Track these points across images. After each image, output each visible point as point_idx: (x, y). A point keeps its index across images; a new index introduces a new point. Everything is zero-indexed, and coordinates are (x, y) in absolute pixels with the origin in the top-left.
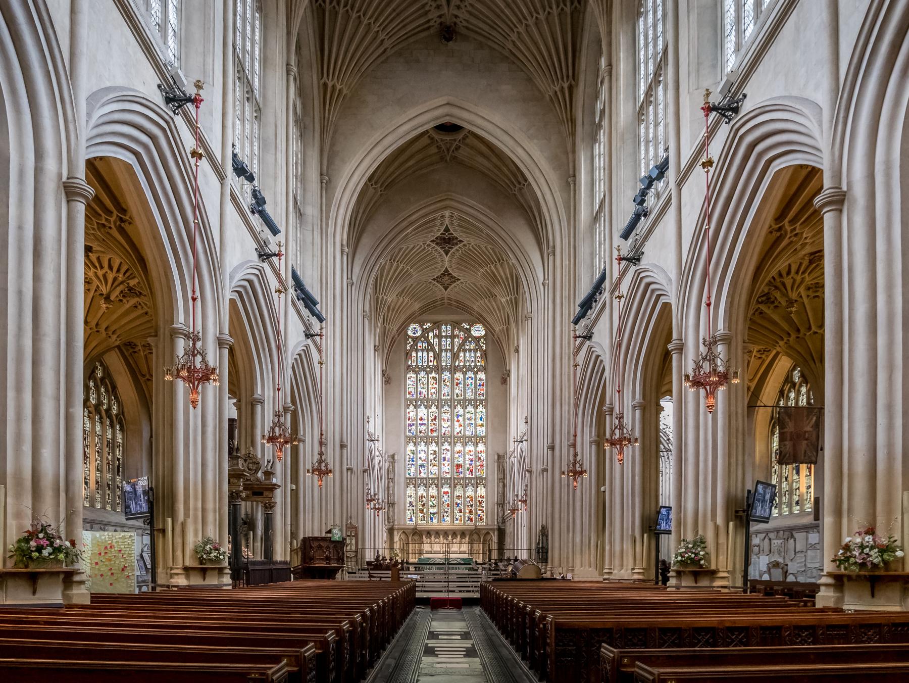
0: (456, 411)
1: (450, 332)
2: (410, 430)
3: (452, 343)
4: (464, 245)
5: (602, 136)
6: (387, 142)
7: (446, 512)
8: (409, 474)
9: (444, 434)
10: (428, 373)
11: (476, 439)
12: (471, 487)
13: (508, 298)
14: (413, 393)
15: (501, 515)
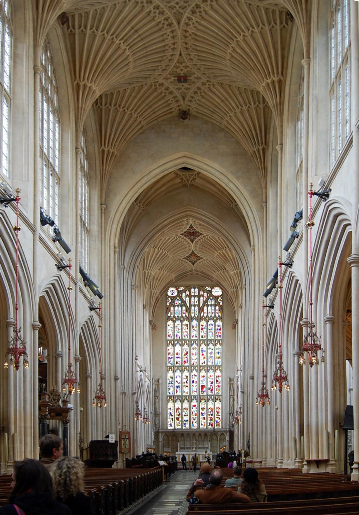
0: (201, 347)
1: (197, 293)
2: (170, 362)
4: (204, 236)
6: (143, 181)
8: (169, 393)
9: (193, 364)
10: (182, 321)
11: (215, 368)
12: (212, 401)
13: (235, 272)
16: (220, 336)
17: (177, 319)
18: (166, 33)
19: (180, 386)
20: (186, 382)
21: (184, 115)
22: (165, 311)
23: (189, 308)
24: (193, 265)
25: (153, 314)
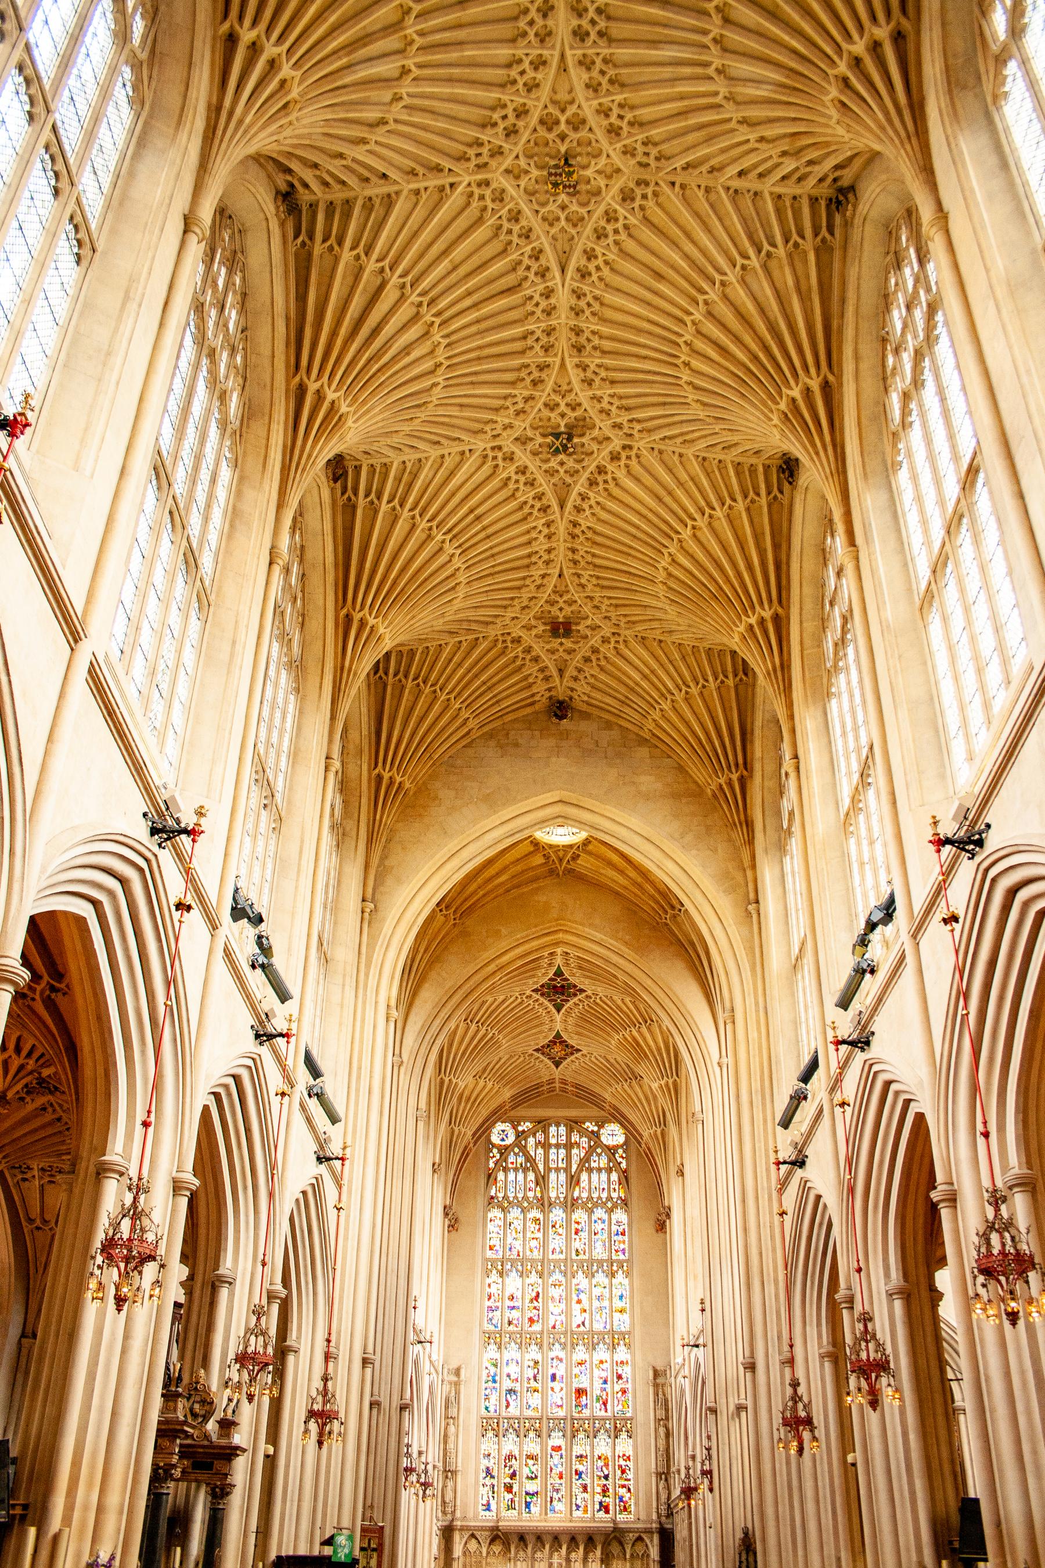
0: (574, 1281)
3: (569, 1157)
7: (557, 1491)
8: (487, 1408)
9: (554, 1327)
11: (614, 1339)
15: (663, 1497)
18: (535, 528)
19: (518, 1389)
20: (535, 1377)
21: (560, 709)
22: (483, 1181)
25: (454, 1188)
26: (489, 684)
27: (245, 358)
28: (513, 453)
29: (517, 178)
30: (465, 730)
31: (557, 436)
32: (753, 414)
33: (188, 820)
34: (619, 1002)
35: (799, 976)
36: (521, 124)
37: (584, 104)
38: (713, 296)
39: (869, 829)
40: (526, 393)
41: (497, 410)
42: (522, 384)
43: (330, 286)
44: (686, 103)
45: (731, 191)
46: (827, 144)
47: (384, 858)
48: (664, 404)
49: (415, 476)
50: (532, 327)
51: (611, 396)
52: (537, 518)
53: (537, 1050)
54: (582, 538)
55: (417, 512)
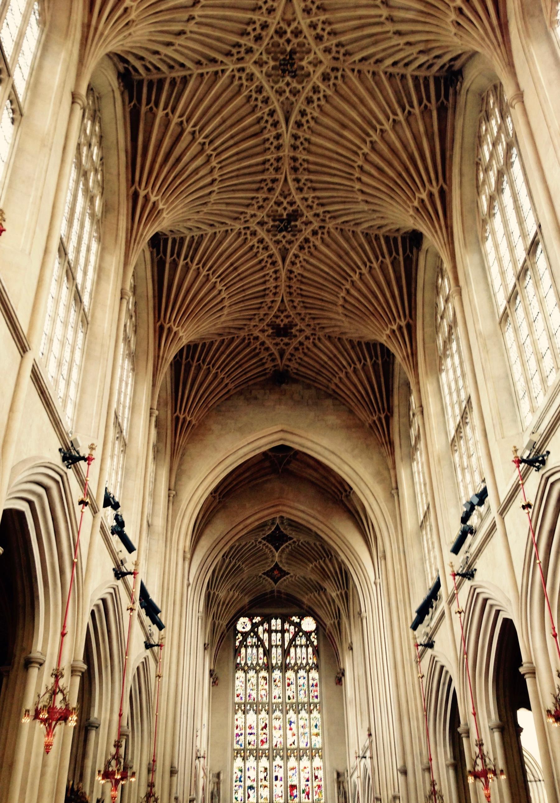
0: (288, 716)
1: (280, 626)
2: (238, 741)
3: (283, 637)
5: (420, 456)
9: (276, 746)
10: (257, 672)
14: (241, 696)
16: (317, 697)
17: (250, 668)
18: (268, 274)
19: (255, 785)
20: (265, 780)
22: (232, 654)
23: (268, 651)
24: (276, 584)
25: (217, 660)
26: (240, 363)
27: (103, 176)
28: (256, 231)
29: (261, 66)
30: (226, 390)
31: (281, 221)
32: (397, 208)
33: (84, 452)
34: (313, 545)
35: (424, 532)
36: (264, 33)
37: (302, 22)
38: (375, 137)
39: (468, 449)
40: (264, 196)
41: (248, 206)
42: (262, 191)
43: (151, 132)
44: (363, 21)
45: (388, 74)
46: (447, 47)
47: (180, 465)
48: (344, 202)
49: (199, 244)
50: (269, 157)
51: (314, 198)
52: (269, 269)
53: (264, 574)
54: (295, 280)
55: (201, 265)
